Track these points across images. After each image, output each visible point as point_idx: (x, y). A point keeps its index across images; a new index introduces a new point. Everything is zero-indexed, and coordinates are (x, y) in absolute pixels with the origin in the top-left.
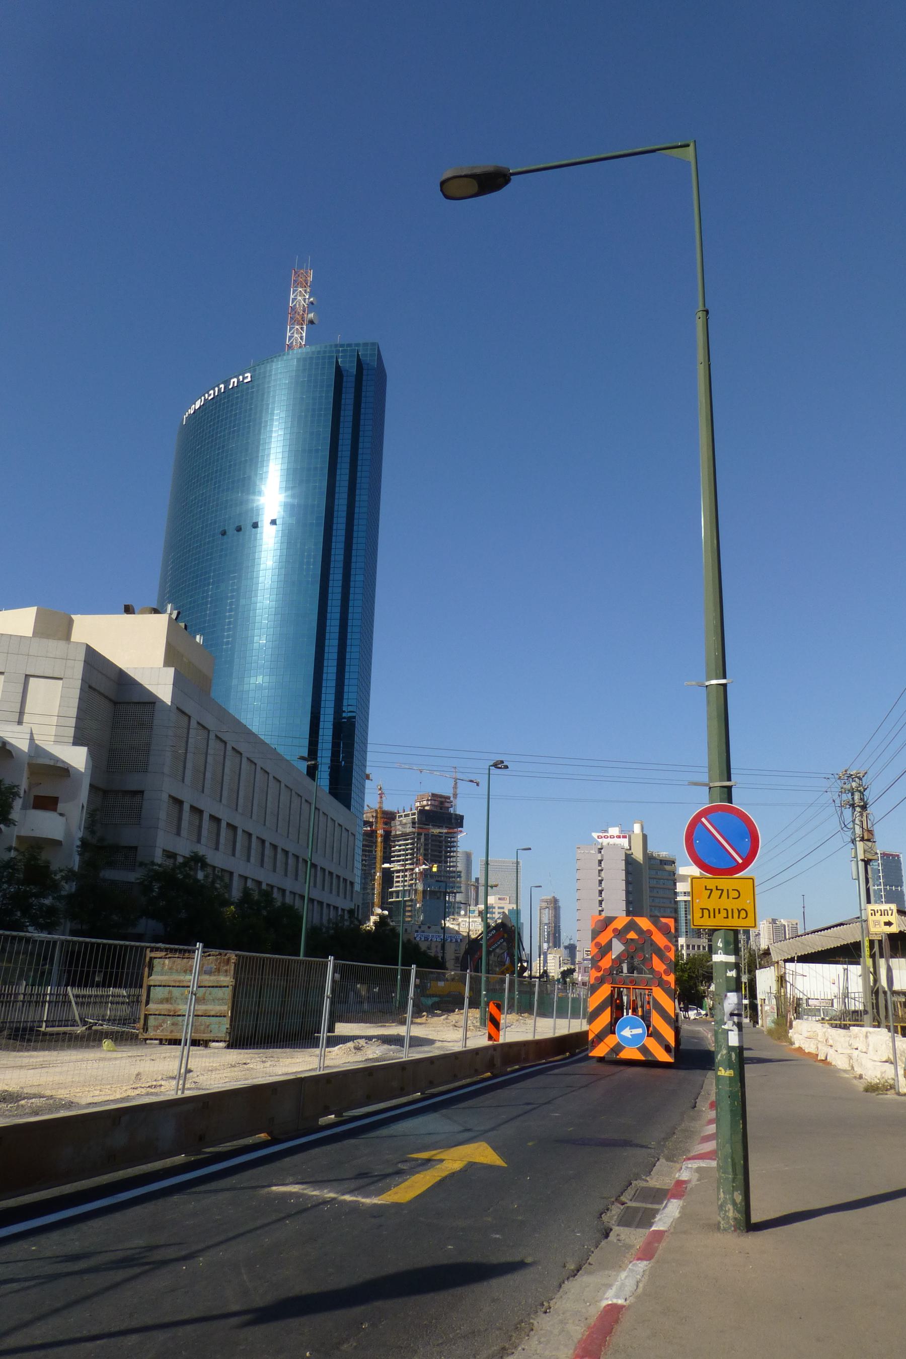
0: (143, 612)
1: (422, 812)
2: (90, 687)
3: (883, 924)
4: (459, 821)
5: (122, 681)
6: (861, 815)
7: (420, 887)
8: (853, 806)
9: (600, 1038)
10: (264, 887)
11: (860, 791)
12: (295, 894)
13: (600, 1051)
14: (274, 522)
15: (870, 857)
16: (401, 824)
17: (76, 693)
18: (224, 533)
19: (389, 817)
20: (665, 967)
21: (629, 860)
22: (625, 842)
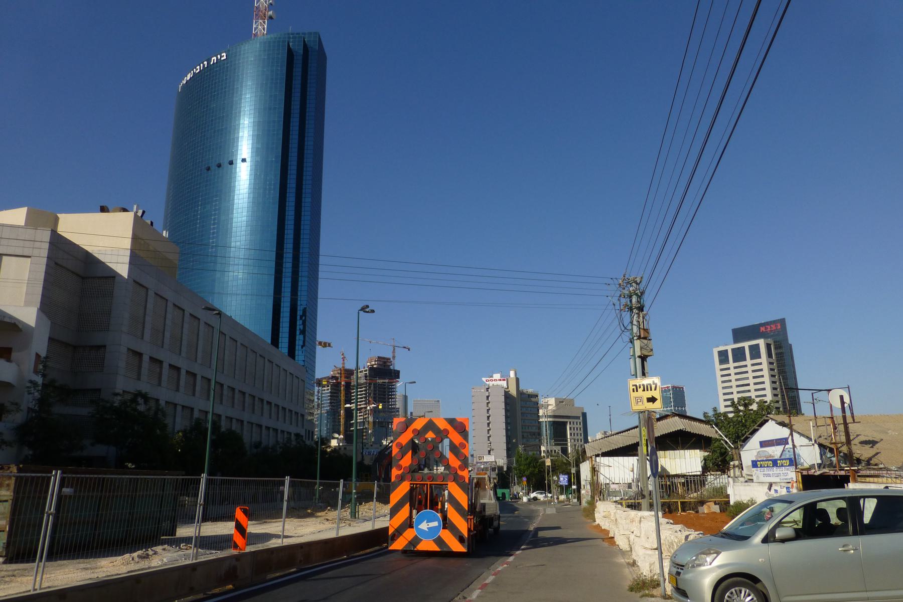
0: (114, 211)
1: (371, 369)
2: (56, 263)
3: (645, 400)
4: (396, 374)
5: (88, 260)
6: (639, 317)
7: (371, 419)
8: (631, 309)
9: (399, 532)
10: (196, 414)
11: (636, 294)
12: (252, 424)
13: (399, 544)
14: (244, 160)
15: (646, 354)
17: (42, 268)
18: (208, 169)
19: (349, 373)
20: (460, 463)
21: (507, 395)
22: (504, 384)
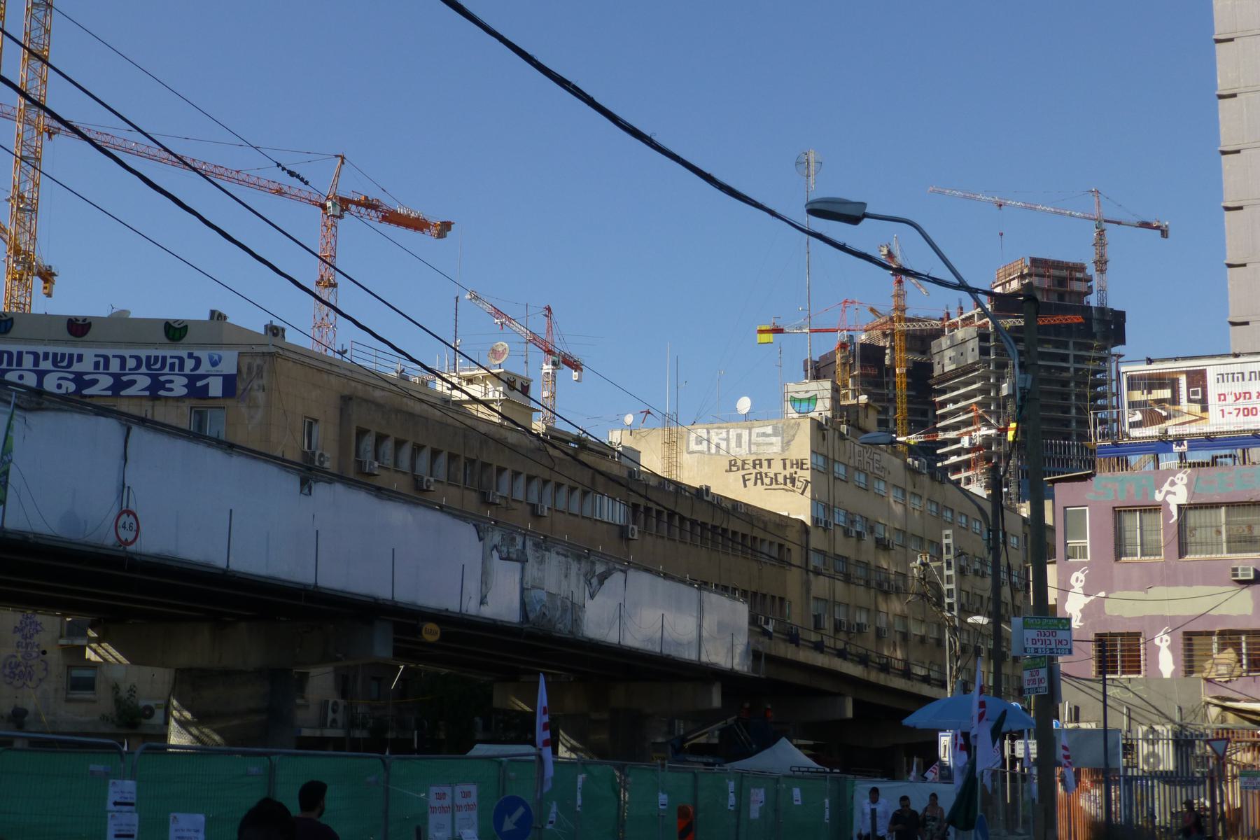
16: (958, 345)
